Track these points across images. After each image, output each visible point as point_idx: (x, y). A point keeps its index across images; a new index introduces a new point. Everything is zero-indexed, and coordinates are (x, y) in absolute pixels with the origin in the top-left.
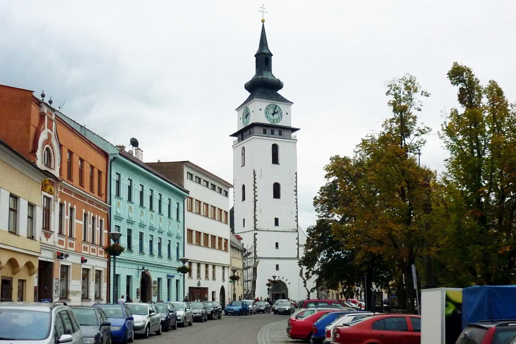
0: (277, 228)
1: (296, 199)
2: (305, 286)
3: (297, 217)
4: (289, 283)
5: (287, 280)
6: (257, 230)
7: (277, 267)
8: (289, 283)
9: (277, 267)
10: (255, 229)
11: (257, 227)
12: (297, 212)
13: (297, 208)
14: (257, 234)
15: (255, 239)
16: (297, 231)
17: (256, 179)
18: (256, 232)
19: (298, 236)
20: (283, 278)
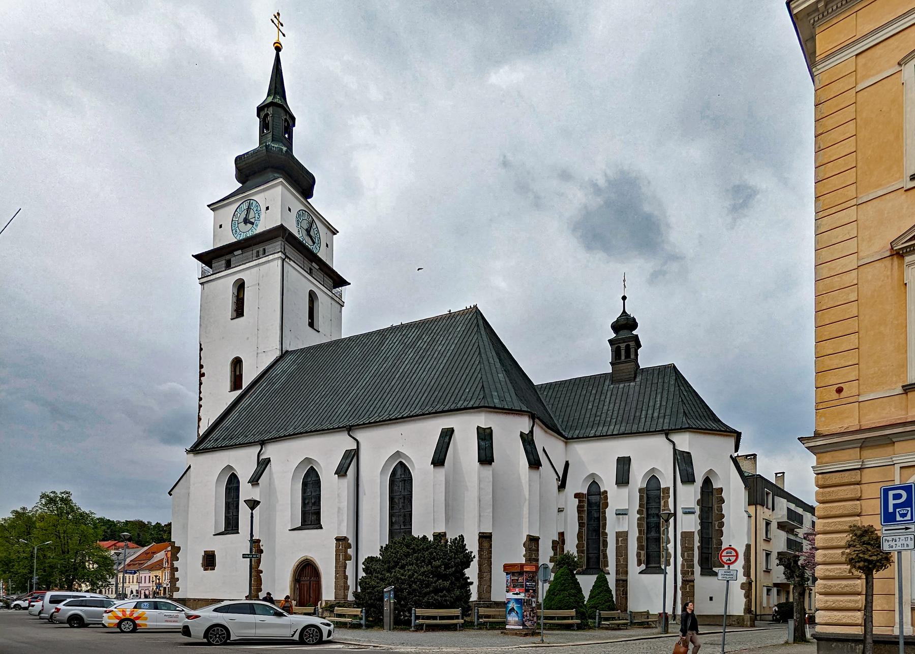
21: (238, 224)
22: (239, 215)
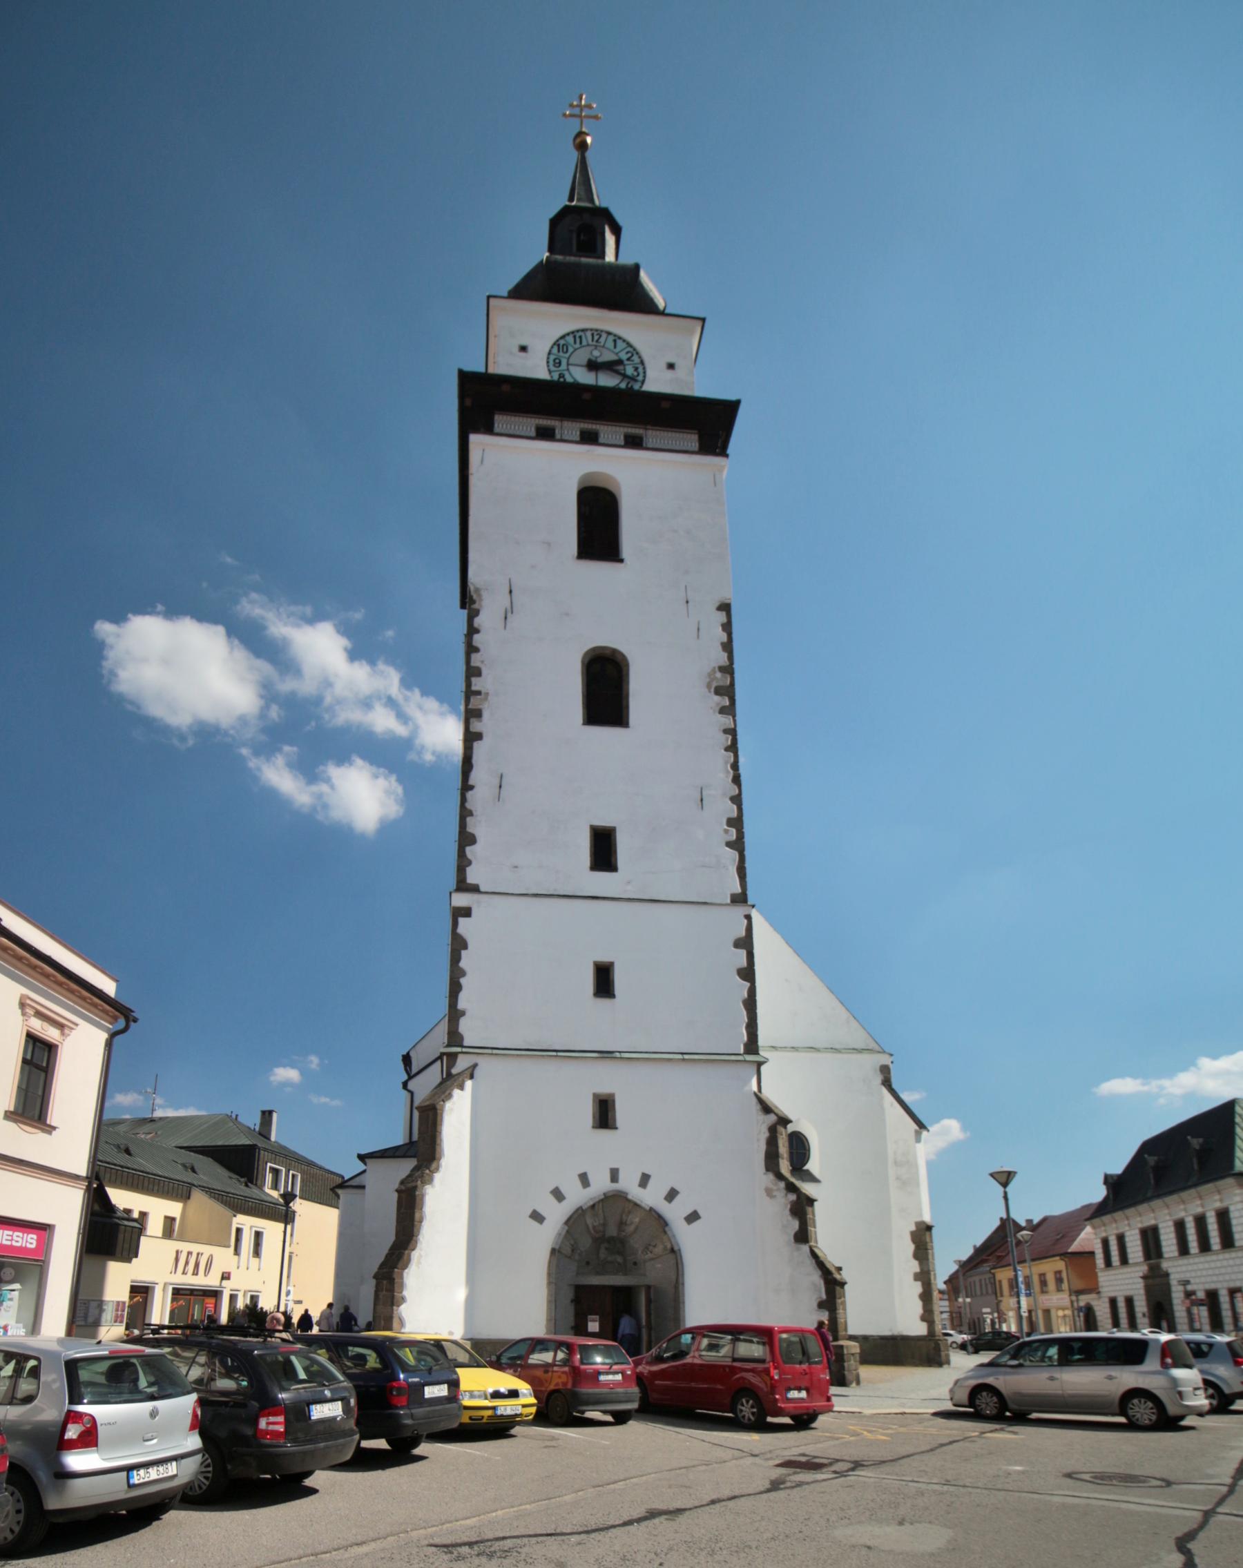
0: (603, 882)
1: (732, 732)
2: (802, 1236)
3: (736, 822)
4: (693, 1217)
5: (672, 1195)
6: (475, 889)
7: (605, 1114)
8: (693, 1217)
9: (605, 1114)
10: (463, 886)
11: (472, 878)
12: (737, 800)
13: (737, 780)
14: (467, 912)
15: (458, 944)
16: (740, 899)
17: (477, 631)
18: (461, 900)
19: (749, 929)
20: (645, 1180)
21: (568, 364)
22: (571, 350)
